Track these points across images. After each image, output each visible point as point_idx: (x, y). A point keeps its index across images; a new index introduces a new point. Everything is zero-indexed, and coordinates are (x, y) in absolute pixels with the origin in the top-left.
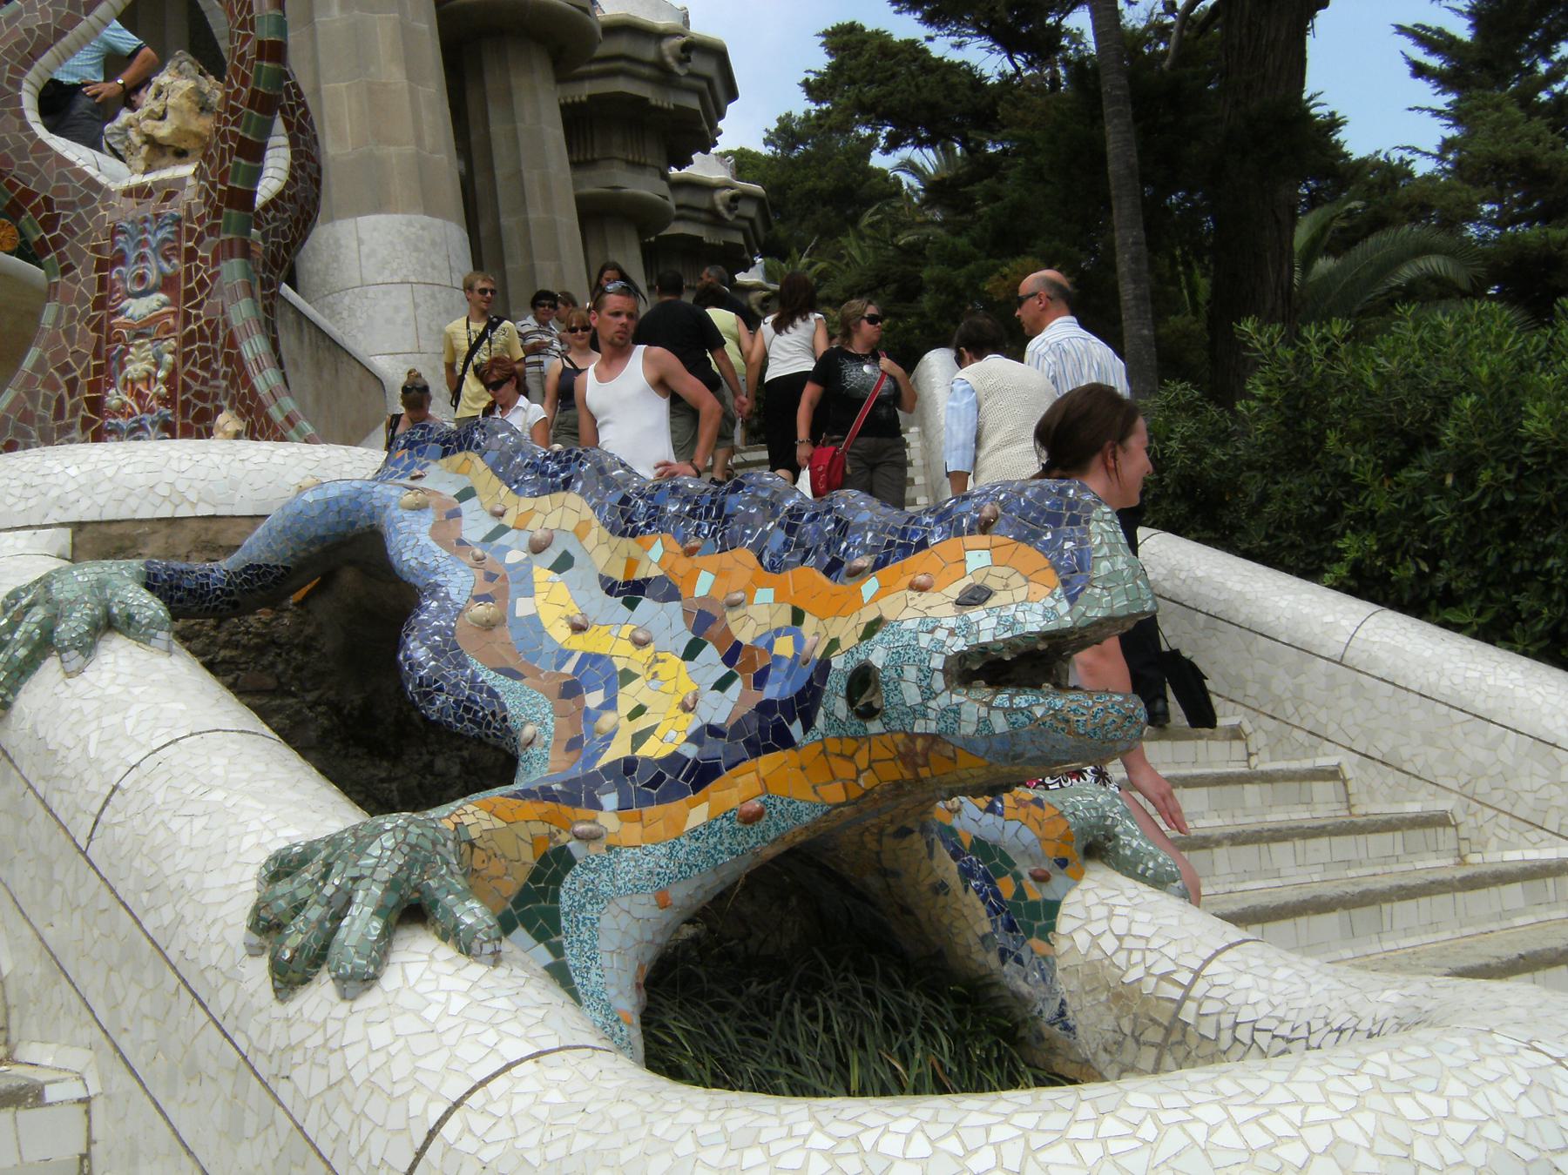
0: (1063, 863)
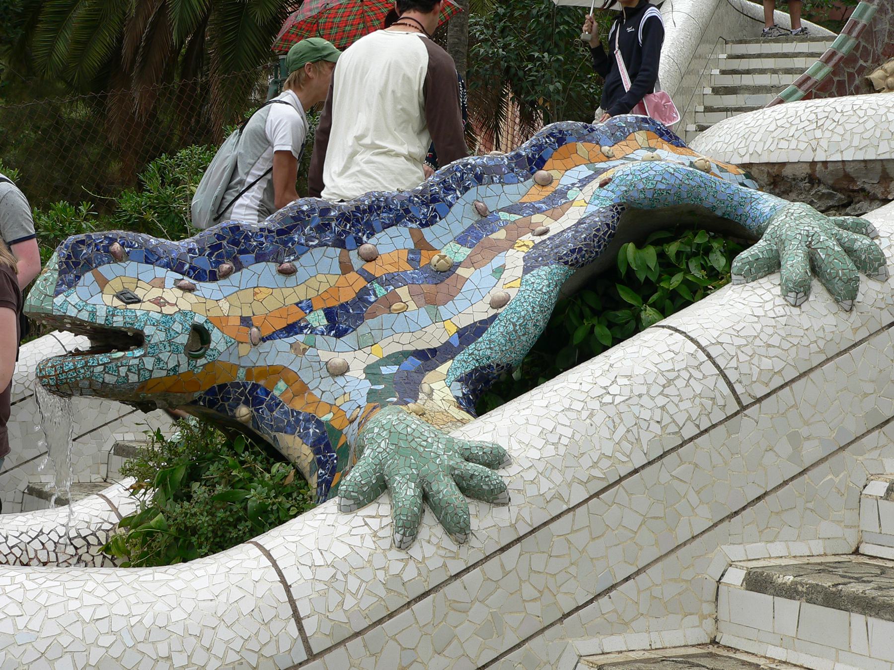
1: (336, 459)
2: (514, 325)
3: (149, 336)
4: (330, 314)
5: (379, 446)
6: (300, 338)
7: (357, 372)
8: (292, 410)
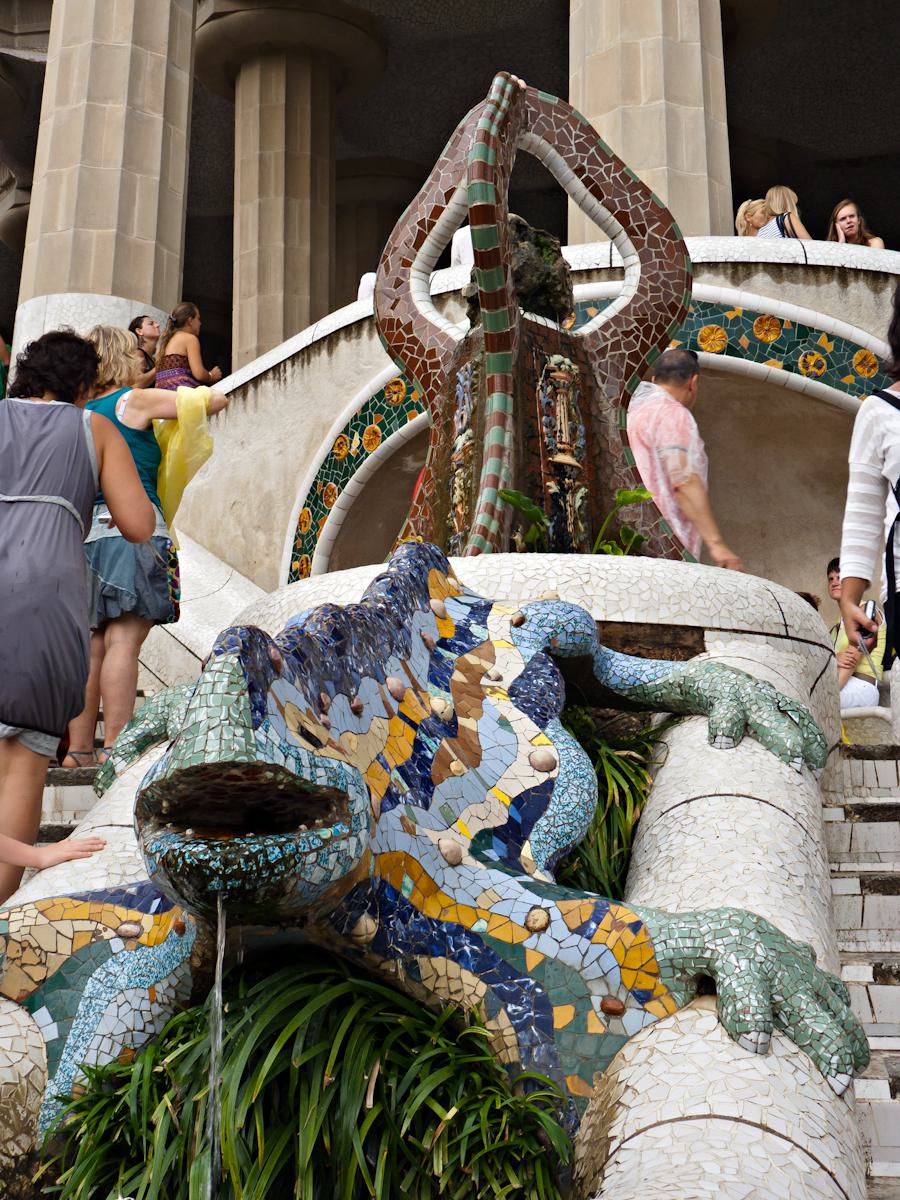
0: (644, 997)
1: (537, 985)
2: (589, 794)
3: (352, 802)
4: (400, 769)
5: (756, 954)
6: (400, 810)
7: (468, 860)
8: (430, 919)
